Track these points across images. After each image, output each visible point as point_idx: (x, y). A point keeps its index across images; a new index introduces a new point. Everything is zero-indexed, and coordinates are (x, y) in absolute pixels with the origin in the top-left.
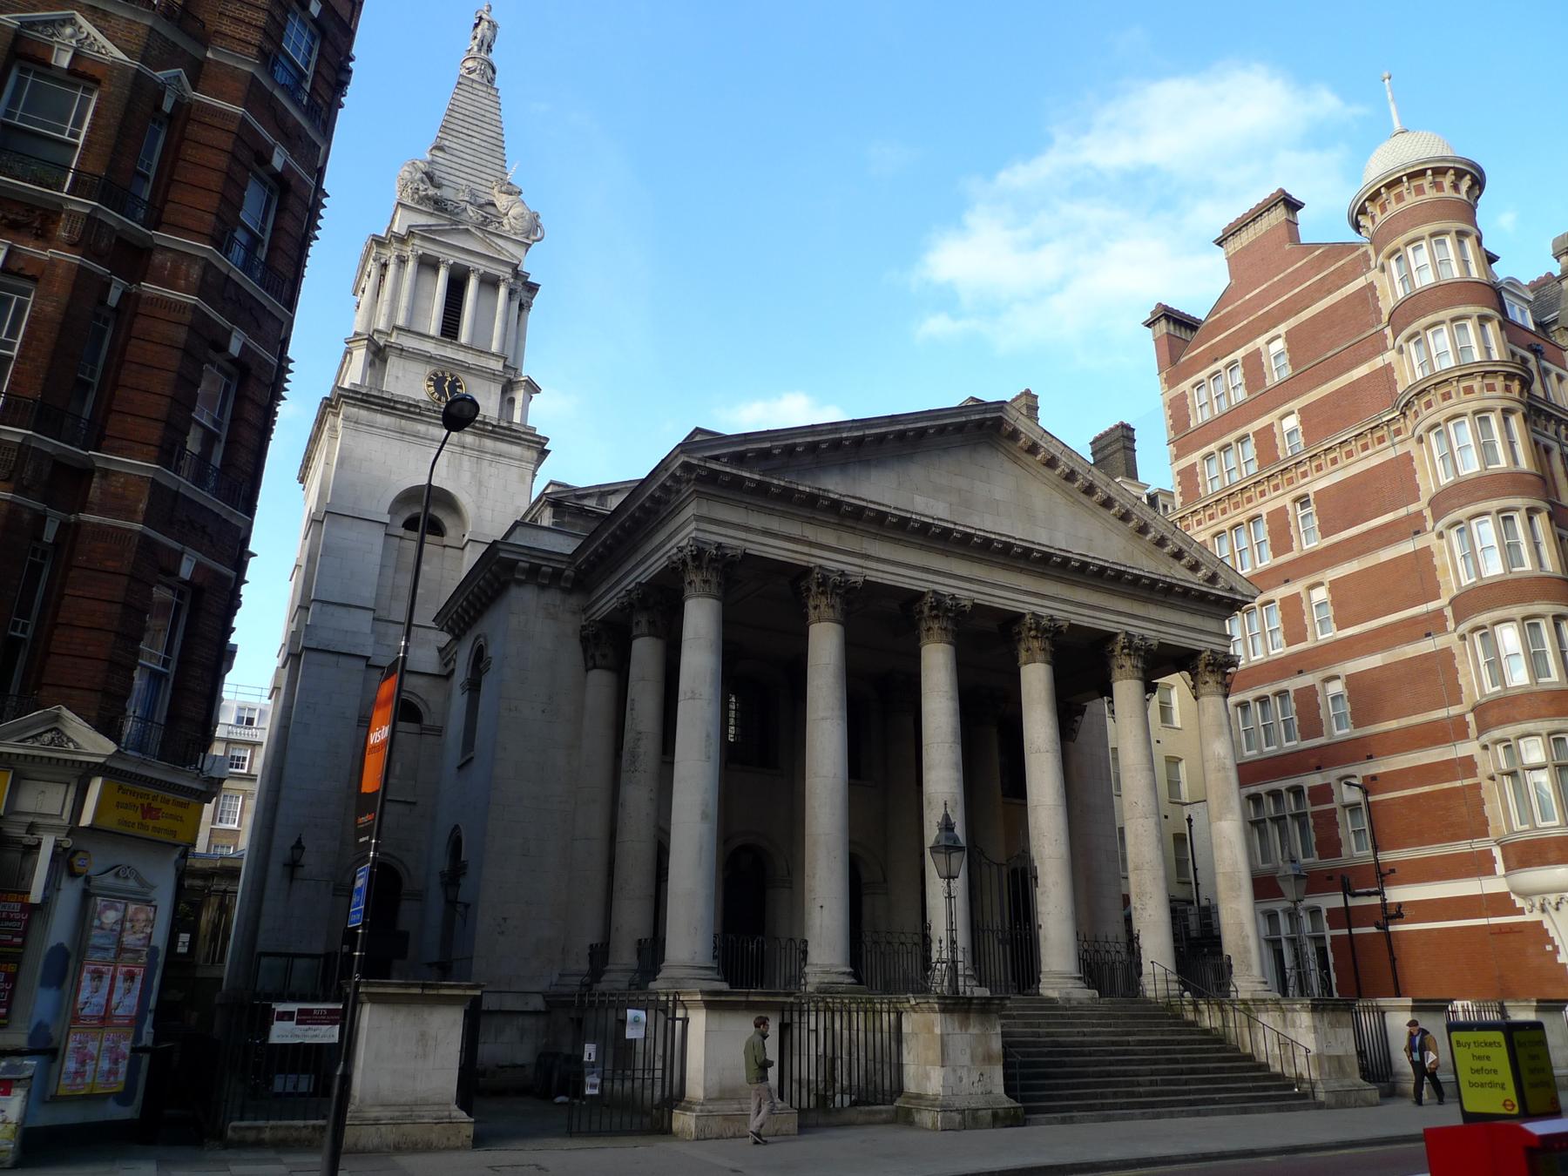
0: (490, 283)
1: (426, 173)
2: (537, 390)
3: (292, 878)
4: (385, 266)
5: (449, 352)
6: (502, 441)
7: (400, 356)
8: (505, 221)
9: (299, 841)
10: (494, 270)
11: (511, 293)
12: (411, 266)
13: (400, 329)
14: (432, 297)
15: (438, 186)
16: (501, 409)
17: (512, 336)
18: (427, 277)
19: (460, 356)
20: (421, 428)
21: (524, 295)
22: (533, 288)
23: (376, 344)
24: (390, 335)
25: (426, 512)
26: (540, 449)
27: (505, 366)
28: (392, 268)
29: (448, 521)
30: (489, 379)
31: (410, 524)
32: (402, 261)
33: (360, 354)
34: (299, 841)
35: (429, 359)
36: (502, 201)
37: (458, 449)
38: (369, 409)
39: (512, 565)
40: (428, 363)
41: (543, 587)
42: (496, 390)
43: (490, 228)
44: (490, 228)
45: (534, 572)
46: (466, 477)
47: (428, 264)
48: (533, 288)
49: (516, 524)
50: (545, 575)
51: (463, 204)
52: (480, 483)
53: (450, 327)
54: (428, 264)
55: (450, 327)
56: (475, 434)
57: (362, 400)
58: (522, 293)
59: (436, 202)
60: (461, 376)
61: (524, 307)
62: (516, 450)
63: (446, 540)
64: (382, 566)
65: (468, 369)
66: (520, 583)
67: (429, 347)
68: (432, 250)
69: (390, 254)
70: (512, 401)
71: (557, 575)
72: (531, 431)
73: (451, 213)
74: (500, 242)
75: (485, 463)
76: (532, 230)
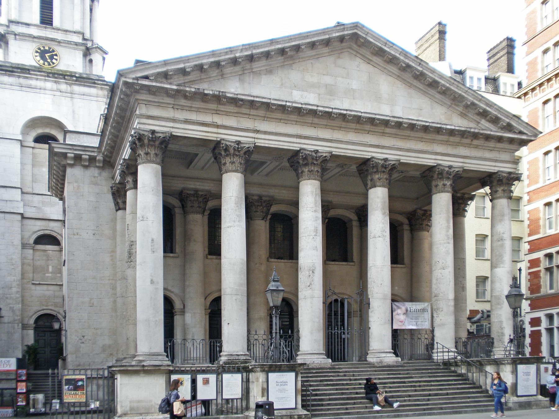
20: (33, 83)
24: (8, 26)
42: (78, 55)
52: (74, 112)
56: (66, 83)
75: (75, 100)
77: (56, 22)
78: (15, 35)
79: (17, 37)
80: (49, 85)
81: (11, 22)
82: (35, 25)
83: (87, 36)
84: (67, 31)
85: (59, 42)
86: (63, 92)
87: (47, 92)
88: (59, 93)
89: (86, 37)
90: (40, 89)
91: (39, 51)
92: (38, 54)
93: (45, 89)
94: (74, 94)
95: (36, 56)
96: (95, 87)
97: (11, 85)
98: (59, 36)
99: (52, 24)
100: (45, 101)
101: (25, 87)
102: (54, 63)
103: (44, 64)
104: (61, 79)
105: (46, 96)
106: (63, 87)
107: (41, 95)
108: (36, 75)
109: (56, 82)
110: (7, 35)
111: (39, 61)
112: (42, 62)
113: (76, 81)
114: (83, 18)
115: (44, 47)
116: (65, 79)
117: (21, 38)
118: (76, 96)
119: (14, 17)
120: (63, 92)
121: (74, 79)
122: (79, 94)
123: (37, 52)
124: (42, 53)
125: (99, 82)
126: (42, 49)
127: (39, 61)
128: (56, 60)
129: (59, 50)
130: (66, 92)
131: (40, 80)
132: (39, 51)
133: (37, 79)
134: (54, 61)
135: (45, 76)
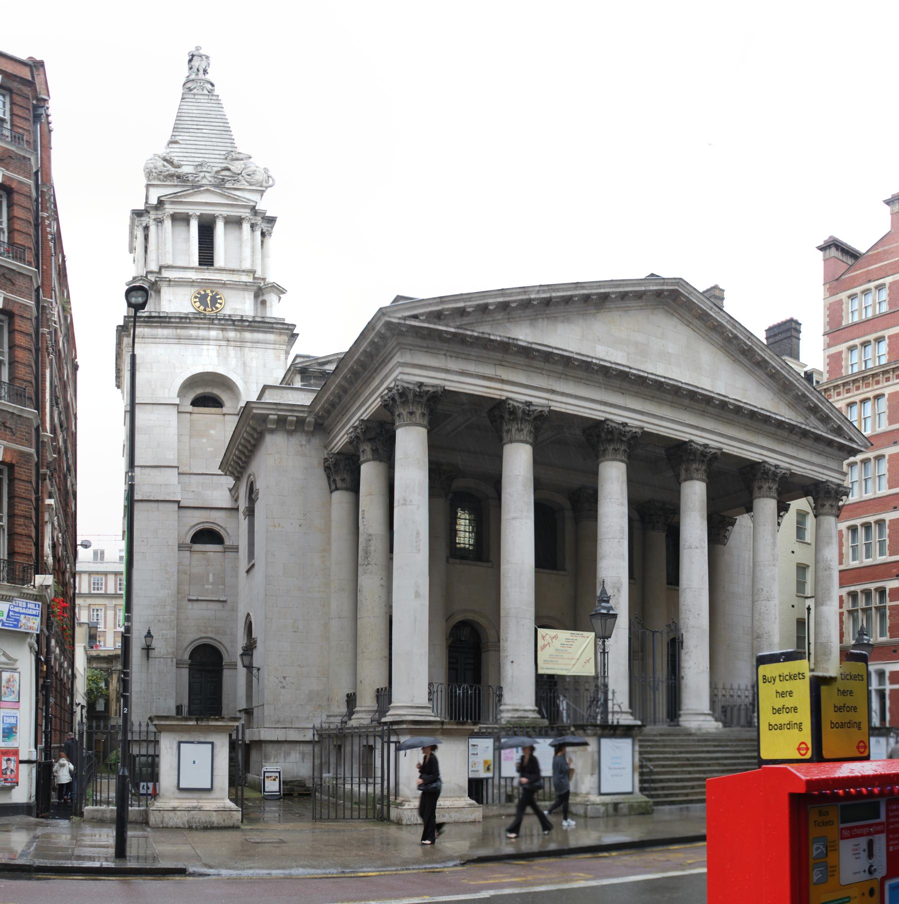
3: (148, 657)
5: (207, 275)
9: (149, 632)
20: (193, 332)
25: (206, 393)
29: (224, 397)
31: (199, 402)
34: (149, 632)
35: (192, 283)
39: (264, 418)
41: (290, 433)
45: (282, 422)
46: (233, 362)
49: (265, 388)
50: (291, 422)
53: (206, 257)
55: (206, 257)
63: (225, 410)
64: (180, 435)
65: (224, 285)
66: (272, 431)
71: (300, 422)
77: (220, 259)
80: (213, 333)
85: (224, 284)
88: (224, 343)
90: (203, 339)
93: (209, 339)
99: (212, 265)
100: (206, 356)
102: (217, 308)
105: (210, 347)
107: (205, 347)
108: (198, 323)
109: (222, 330)
112: (202, 308)
115: (205, 291)
123: (196, 297)
124: (202, 299)
126: (203, 293)
128: (220, 304)
129: (225, 293)
131: (203, 328)
133: (199, 328)
134: (218, 305)
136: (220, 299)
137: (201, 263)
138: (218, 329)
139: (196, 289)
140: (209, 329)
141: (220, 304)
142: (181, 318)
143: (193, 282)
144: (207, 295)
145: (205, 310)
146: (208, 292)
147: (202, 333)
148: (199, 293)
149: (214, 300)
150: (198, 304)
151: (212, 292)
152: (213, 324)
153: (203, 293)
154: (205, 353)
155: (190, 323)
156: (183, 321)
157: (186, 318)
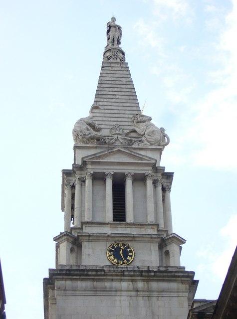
0: (140, 179)
1: (89, 124)
2: (183, 241)
4: (73, 187)
5: (120, 230)
6: (163, 281)
7: (89, 241)
8: (143, 138)
10: (140, 170)
11: (155, 183)
12: (89, 182)
13: (87, 223)
14: (104, 197)
15: (99, 130)
16: (161, 260)
17: (161, 210)
18: (98, 187)
19: (128, 231)
20: (107, 284)
21: (165, 181)
22: (169, 176)
23: (73, 237)
24: (81, 229)
26: (190, 281)
27: (158, 231)
28: (77, 187)
30: (150, 242)
32: (83, 181)
33: (64, 246)
36: (140, 128)
37: (133, 294)
38: (72, 280)
40: (107, 240)
42: (155, 248)
43: (134, 146)
44: (134, 146)
47: (99, 178)
48: (169, 176)
51: (115, 137)
53: (119, 214)
54: (99, 178)
55: (119, 214)
56: (144, 281)
57: (66, 275)
58: (163, 181)
59: (98, 140)
60: (130, 244)
61: (165, 190)
62: (174, 285)
65: (133, 238)
67: (108, 230)
68: (99, 169)
69: (75, 179)
70: (167, 253)
72: (182, 270)
73: (109, 144)
74: (142, 153)
75: (154, 299)
76: (160, 142)
77: (130, 217)
78: (89, 236)
79: (91, 238)
80: (124, 285)
81: (83, 223)
82: (108, 224)
83: (162, 227)
84: (141, 225)
85: (134, 237)
86: (141, 291)
87: (123, 293)
89: (160, 229)
90: (116, 291)
91: (113, 249)
92: (111, 253)
93: (121, 291)
94: (153, 291)
95: (110, 256)
96: (175, 281)
97: (85, 290)
98: (134, 231)
99: (124, 220)
101: (100, 291)
102: (128, 261)
103: (118, 263)
104: (138, 276)
105: (123, 298)
106: (140, 285)
107: (117, 298)
109: (133, 281)
110: (80, 238)
111: (113, 260)
112: (116, 260)
113: (154, 276)
114: (156, 210)
115: (118, 245)
116: (142, 276)
117: (95, 238)
118: (155, 294)
119: (87, 218)
120: (141, 291)
121: (153, 274)
122: (157, 292)
123: (110, 251)
124: (115, 252)
125: (180, 274)
126: (116, 246)
127: (113, 260)
128: (131, 256)
129: (135, 246)
130: (144, 291)
132: (113, 249)
133: (112, 280)
134: (129, 258)
135: (121, 276)
136: (131, 251)
137: (115, 219)
138: (129, 280)
139: (111, 243)
140: (121, 280)
141: (131, 256)
142: (97, 271)
143: (108, 236)
144: (119, 248)
145: (118, 263)
146: (121, 245)
147: (116, 284)
148: (113, 247)
149: (126, 253)
150: (112, 257)
151: (124, 245)
152: (124, 275)
153: (116, 246)
154: (118, 303)
155: (104, 275)
156: (97, 274)
157: (101, 270)
